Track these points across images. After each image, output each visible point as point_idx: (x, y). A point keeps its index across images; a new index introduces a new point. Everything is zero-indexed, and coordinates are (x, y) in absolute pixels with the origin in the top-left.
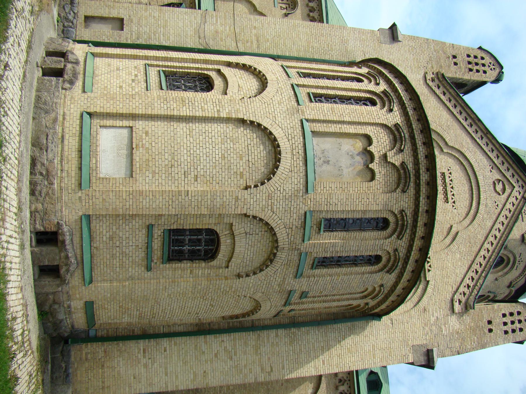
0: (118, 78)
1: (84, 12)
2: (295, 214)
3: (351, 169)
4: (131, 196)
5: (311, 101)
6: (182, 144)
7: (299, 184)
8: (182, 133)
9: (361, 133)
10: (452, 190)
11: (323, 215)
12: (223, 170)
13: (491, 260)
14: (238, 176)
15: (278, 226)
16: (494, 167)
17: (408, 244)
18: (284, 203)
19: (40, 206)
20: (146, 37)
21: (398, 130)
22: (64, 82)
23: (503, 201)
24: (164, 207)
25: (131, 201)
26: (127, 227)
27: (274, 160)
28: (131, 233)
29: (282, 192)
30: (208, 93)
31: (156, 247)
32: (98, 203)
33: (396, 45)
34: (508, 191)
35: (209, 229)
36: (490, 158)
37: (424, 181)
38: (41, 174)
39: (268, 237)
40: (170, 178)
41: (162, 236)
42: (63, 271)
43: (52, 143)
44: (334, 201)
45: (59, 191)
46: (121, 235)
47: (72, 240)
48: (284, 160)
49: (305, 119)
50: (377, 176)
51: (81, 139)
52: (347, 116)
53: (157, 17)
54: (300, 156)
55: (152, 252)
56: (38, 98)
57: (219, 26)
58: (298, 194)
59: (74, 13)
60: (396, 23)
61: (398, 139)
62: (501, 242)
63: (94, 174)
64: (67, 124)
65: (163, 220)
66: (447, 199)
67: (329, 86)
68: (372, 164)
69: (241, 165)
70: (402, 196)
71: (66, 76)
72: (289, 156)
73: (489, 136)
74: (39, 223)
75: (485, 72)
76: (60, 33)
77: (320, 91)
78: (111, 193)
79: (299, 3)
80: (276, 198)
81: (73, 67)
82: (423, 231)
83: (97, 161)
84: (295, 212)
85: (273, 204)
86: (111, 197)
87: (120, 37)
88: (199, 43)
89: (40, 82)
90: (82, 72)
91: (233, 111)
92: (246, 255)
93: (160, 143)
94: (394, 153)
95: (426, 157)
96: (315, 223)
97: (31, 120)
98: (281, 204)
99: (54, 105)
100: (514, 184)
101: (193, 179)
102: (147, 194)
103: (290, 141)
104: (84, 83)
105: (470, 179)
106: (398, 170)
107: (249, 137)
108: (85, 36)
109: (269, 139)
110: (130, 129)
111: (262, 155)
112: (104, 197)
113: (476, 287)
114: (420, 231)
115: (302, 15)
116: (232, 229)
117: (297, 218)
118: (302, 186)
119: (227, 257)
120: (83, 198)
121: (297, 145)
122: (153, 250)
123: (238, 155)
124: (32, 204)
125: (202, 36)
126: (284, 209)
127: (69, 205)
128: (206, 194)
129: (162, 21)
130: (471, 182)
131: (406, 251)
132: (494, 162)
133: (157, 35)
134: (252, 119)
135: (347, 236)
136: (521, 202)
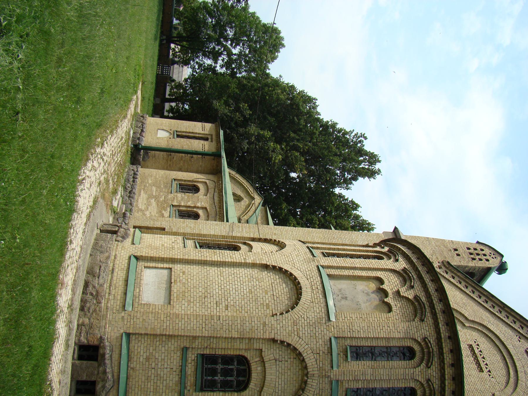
2: (320, 340)
3: (368, 304)
4: (168, 318)
6: (214, 281)
7: (321, 313)
8: (214, 273)
11: (348, 342)
12: (251, 302)
14: (265, 307)
15: (305, 351)
16: (521, 337)
17: (439, 374)
18: (309, 329)
19: (87, 321)
21: (406, 273)
24: (198, 329)
25: (168, 322)
26: (163, 348)
27: (296, 295)
28: (166, 354)
29: (305, 319)
31: (189, 373)
32: (138, 323)
35: (239, 355)
36: (515, 329)
37: (439, 310)
38: (92, 294)
39: (297, 365)
40: (203, 307)
41: (195, 360)
42: (99, 387)
43: (104, 272)
44: (356, 328)
45: (105, 310)
46: (157, 357)
47: (111, 356)
48: (305, 294)
49: (321, 266)
50: (394, 308)
51: (128, 273)
53: (193, 227)
54: (319, 291)
55: (185, 377)
56: (96, 244)
58: (321, 321)
59: (125, 223)
63: (137, 300)
65: (197, 344)
66: (481, 369)
68: (387, 299)
69: (267, 298)
70: (422, 325)
71: (119, 234)
72: (309, 290)
73: (506, 309)
74: (84, 336)
75: (487, 260)
78: (150, 315)
80: (301, 324)
82: (450, 357)
83: (140, 291)
84: (320, 337)
85: (298, 330)
86: (150, 318)
92: (277, 384)
93: (195, 280)
95: (436, 290)
96: (341, 350)
97: (89, 255)
98: (306, 329)
99: (108, 248)
101: (224, 308)
102: (183, 317)
103: (309, 280)
105: (500, 350)
106: (413, 303)
107: (272, 277)
109: (290, 279)
110: (169, 270)
111: (285, 291)
112: (144, 318)
114: (448, 358)
116: (261, 356)
117: (323, 343)
118: (323, 314)
119: (259, 386)
120: (125, 318)
121: (315, 283)
122: (187, 375)
123: (264, 290)
124: (80, 318)
126: (309, 335)
127: (113, 323)
128: (236, 319)
129: (197, 230)
130: (501, 352)
131: (439, 382)
132: (519, 332)
134: (274, 264)
135: (375, 366)
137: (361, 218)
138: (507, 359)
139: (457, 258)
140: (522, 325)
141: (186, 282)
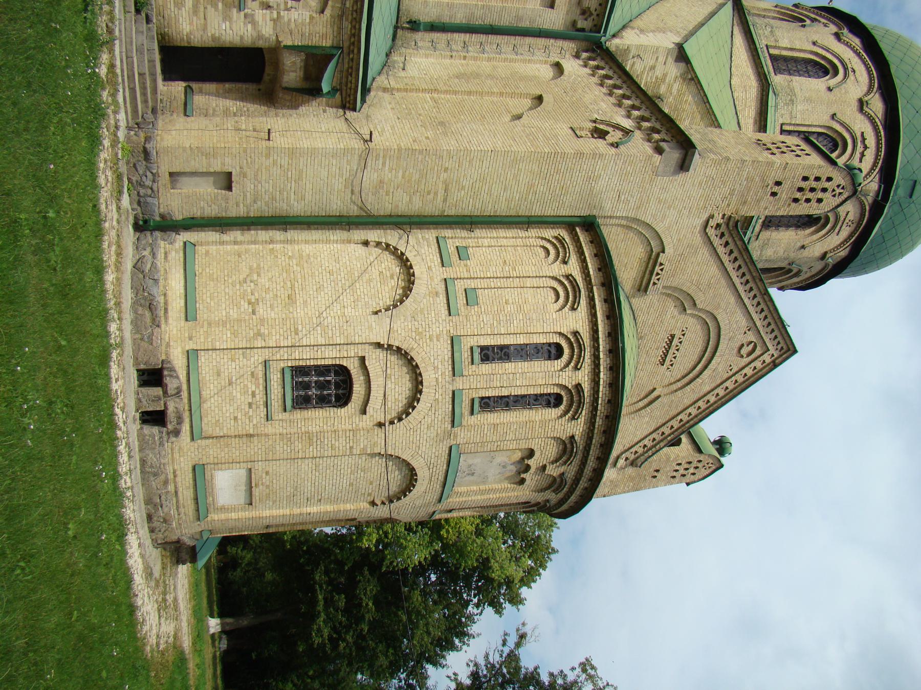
0: (232, 403)
1: (167, 166)
5: (472, 413)
13: (687, 425)
20: (267, 199)
22: (168, 433)
23: (743, 364)
27: (408, 482)
30: (343, 409)
34: (758, 352)
56: (143, 462)
57: (387, 172)
59: (152, 173)
62: (711, 409)
64: (178, 479)
66: (664, 361)
72: (427, 481)
76: (136, 206)
81: (176, 408)
87: (227, 200)
88: (352, 201)
89: (141, 437)
90: (187, 408)
91: (369, 446)
95: (594, 470)
99: (162, 466)
103: (431, 470)
104: (191, 427)
108: (172, 203)
113: (654, 449)
125: (357, 190)
129: (294, 172)
130: (708, 344)
132: (754, 323)
133: (285, 193)
138: (707, 353)
141: (271, 484)
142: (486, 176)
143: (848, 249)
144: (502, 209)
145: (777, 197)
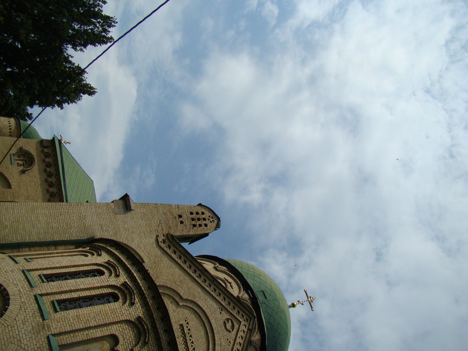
5: (56, 311)
9: (107, 334)
10: (191, 338)
16: (223, 309)
23: (234, 337)
33: (129, 214)
34: (236, 326)
36: (219, 302)
49: (52, 335)
52: (92, 320)
60: (128, 194)
61: (142, 332)
67: (72, 289)
73: (215, 282)
77: (64, 297)
79: (36, 159)
94: (140, 347)
95: (169, 343)
100: (240, 320)
105: (204, 325)
115: (39, 171)
130: (205, 327)
132: (222, 305)
136: (248, 334)
137: (85, 82)
138: (209, 334)
139: (180, 226)
140: (225, 297)
142: (18, 218)
143: (258, 332)
144: (35, 238)
145: (184, 224)
